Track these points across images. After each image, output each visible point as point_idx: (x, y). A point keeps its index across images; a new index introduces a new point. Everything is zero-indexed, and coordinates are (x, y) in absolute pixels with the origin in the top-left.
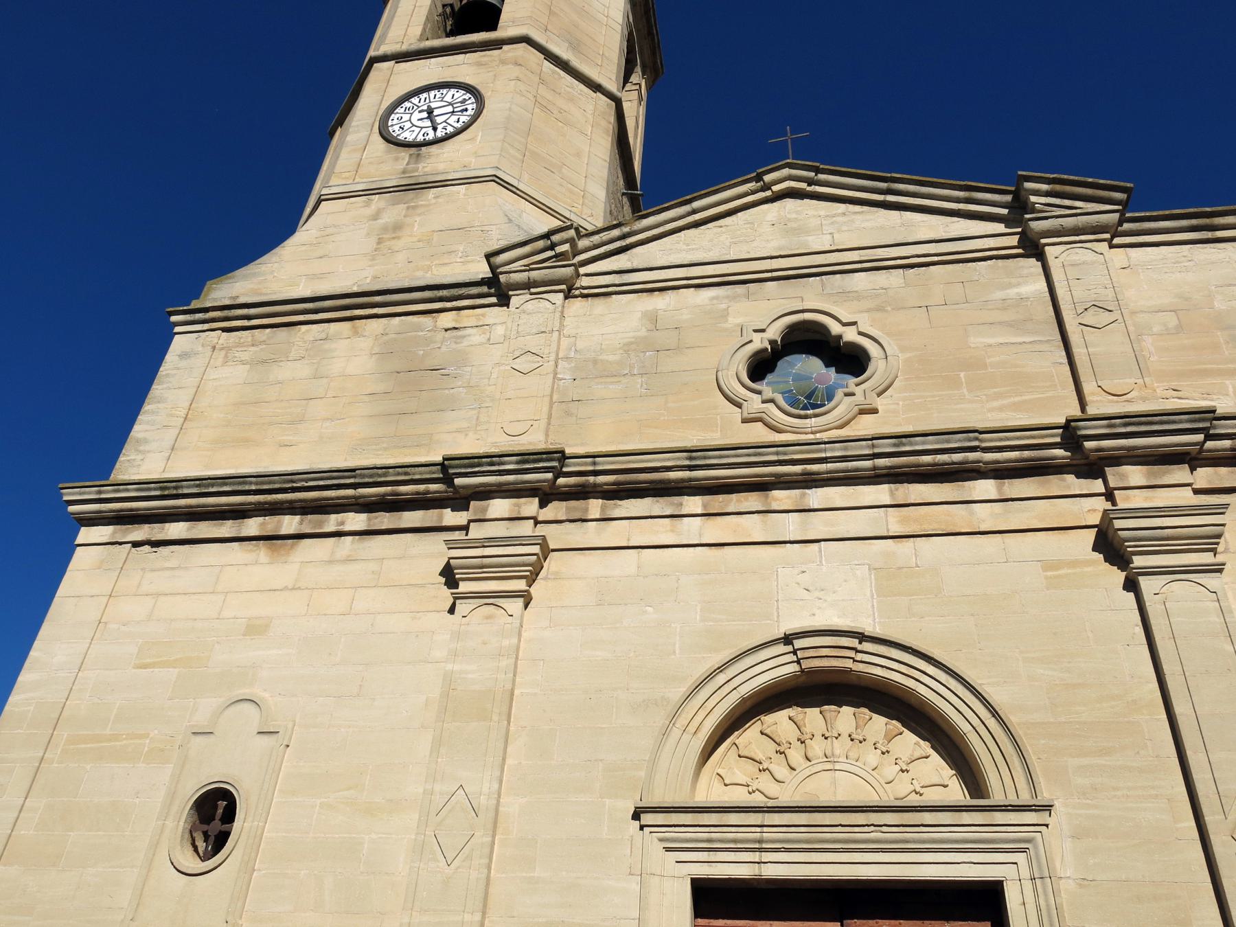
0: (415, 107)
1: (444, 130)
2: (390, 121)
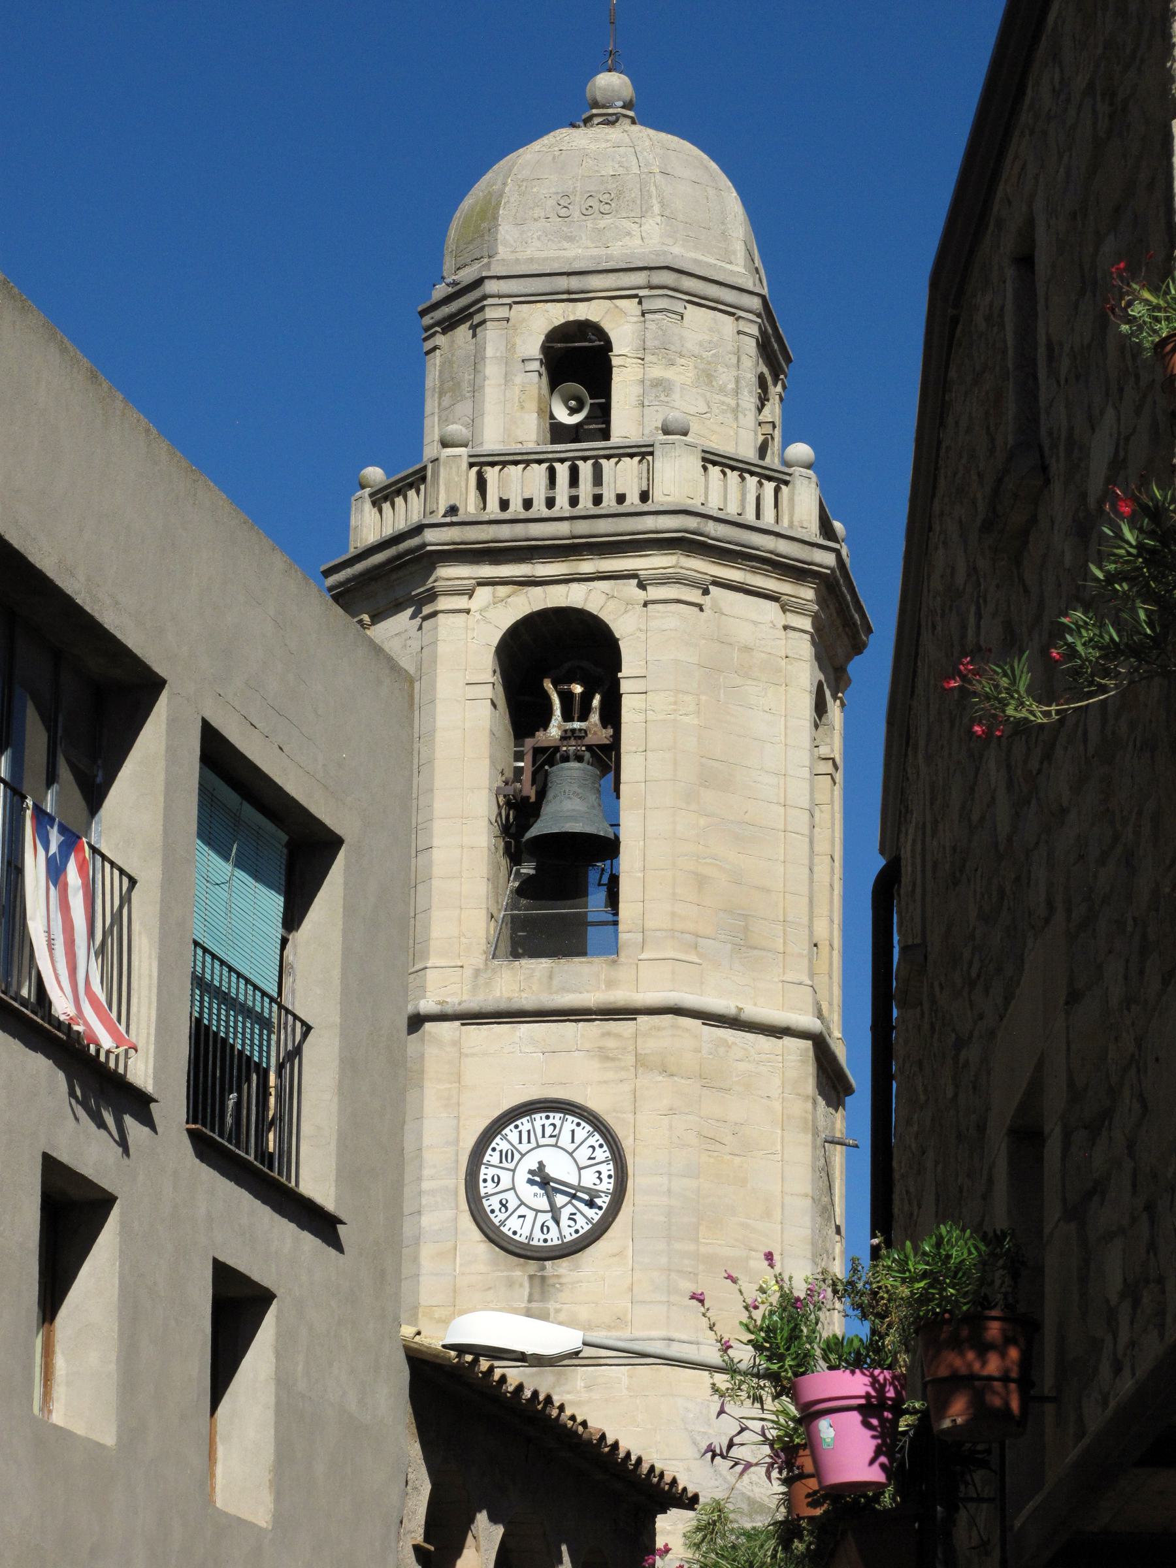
0: (517, 1156)
1: (572, 1223)
2: (482, 1184)
